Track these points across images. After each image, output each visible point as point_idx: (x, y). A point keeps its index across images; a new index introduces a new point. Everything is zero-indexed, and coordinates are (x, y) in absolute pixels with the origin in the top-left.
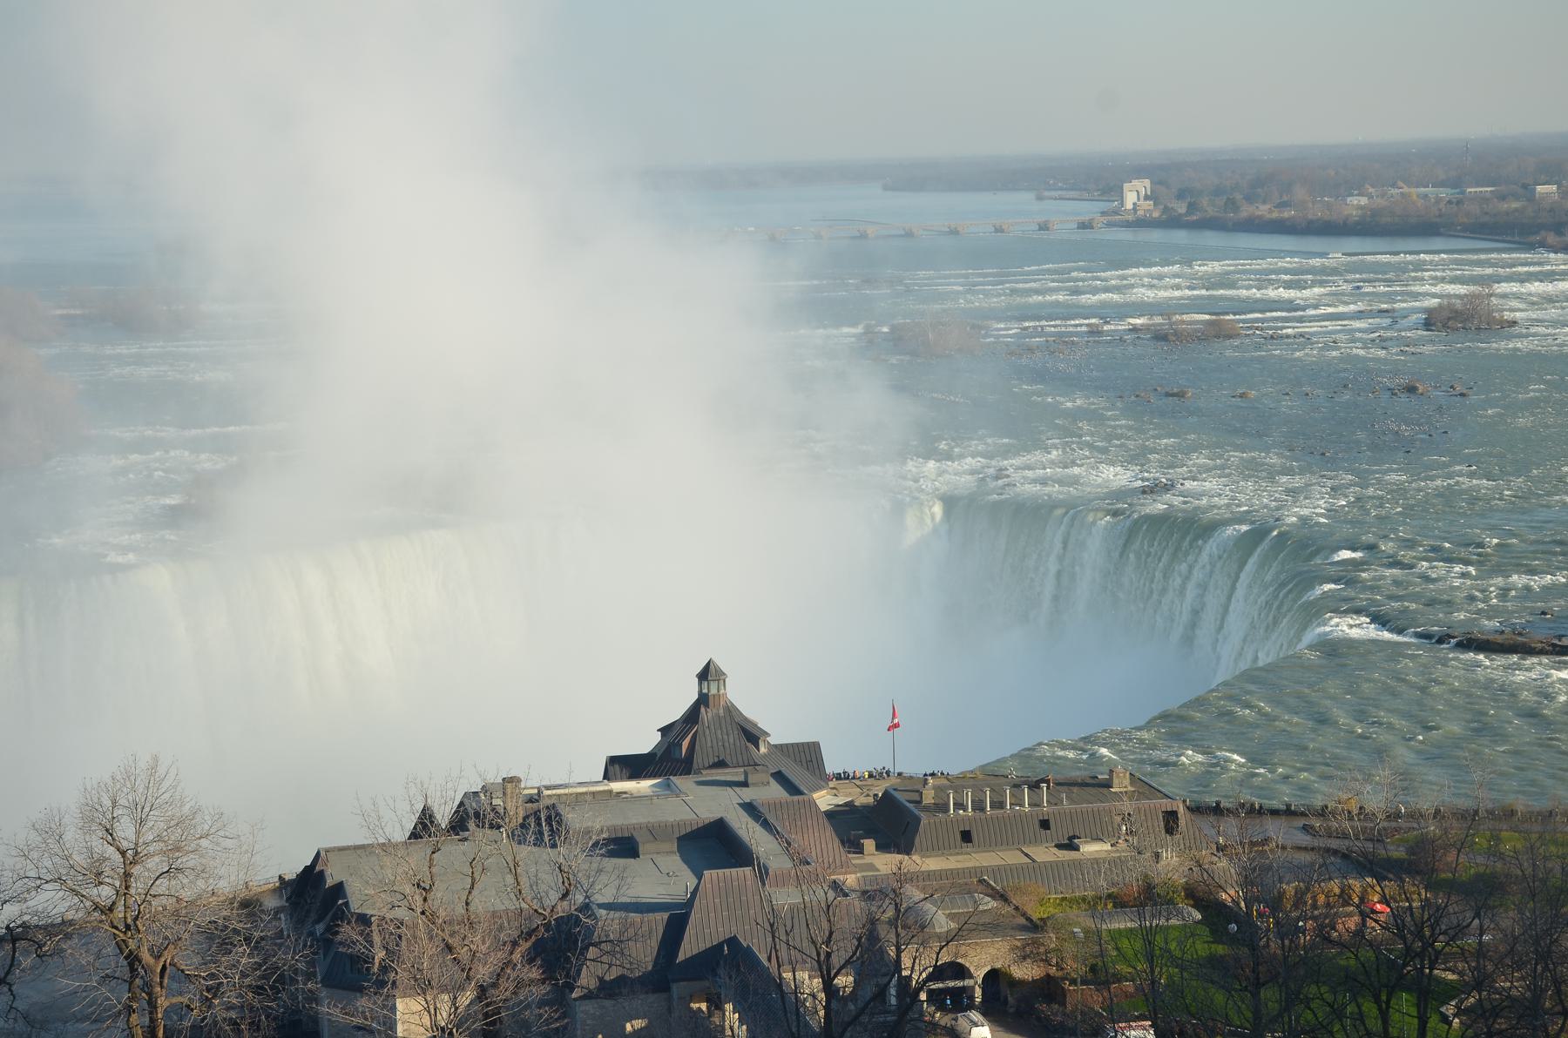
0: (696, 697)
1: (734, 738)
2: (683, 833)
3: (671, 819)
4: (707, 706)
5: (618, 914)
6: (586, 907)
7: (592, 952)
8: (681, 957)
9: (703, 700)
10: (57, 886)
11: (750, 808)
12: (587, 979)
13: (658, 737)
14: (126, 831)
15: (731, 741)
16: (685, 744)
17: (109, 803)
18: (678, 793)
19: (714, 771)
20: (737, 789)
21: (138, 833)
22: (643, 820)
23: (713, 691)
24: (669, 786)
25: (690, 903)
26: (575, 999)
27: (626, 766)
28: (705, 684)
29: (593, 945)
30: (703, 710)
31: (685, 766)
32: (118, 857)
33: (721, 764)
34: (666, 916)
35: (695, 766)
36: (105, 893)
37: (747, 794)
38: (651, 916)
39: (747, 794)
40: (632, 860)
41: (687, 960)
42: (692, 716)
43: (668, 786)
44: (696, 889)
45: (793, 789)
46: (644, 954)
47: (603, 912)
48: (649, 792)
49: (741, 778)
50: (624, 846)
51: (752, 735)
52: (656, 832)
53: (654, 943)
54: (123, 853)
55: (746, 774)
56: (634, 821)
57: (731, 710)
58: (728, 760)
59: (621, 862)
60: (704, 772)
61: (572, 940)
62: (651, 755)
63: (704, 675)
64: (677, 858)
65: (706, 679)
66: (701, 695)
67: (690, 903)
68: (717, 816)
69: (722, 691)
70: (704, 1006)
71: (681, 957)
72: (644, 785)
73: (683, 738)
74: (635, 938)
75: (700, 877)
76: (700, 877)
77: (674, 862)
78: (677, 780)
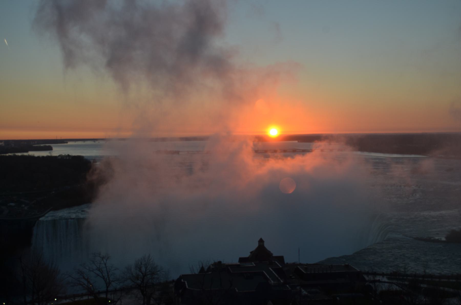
14: (143, 269)
17: (140, 263)
21: (146, 270)
32: (142, 275)
36: (139, 282)
54: (143, 274)
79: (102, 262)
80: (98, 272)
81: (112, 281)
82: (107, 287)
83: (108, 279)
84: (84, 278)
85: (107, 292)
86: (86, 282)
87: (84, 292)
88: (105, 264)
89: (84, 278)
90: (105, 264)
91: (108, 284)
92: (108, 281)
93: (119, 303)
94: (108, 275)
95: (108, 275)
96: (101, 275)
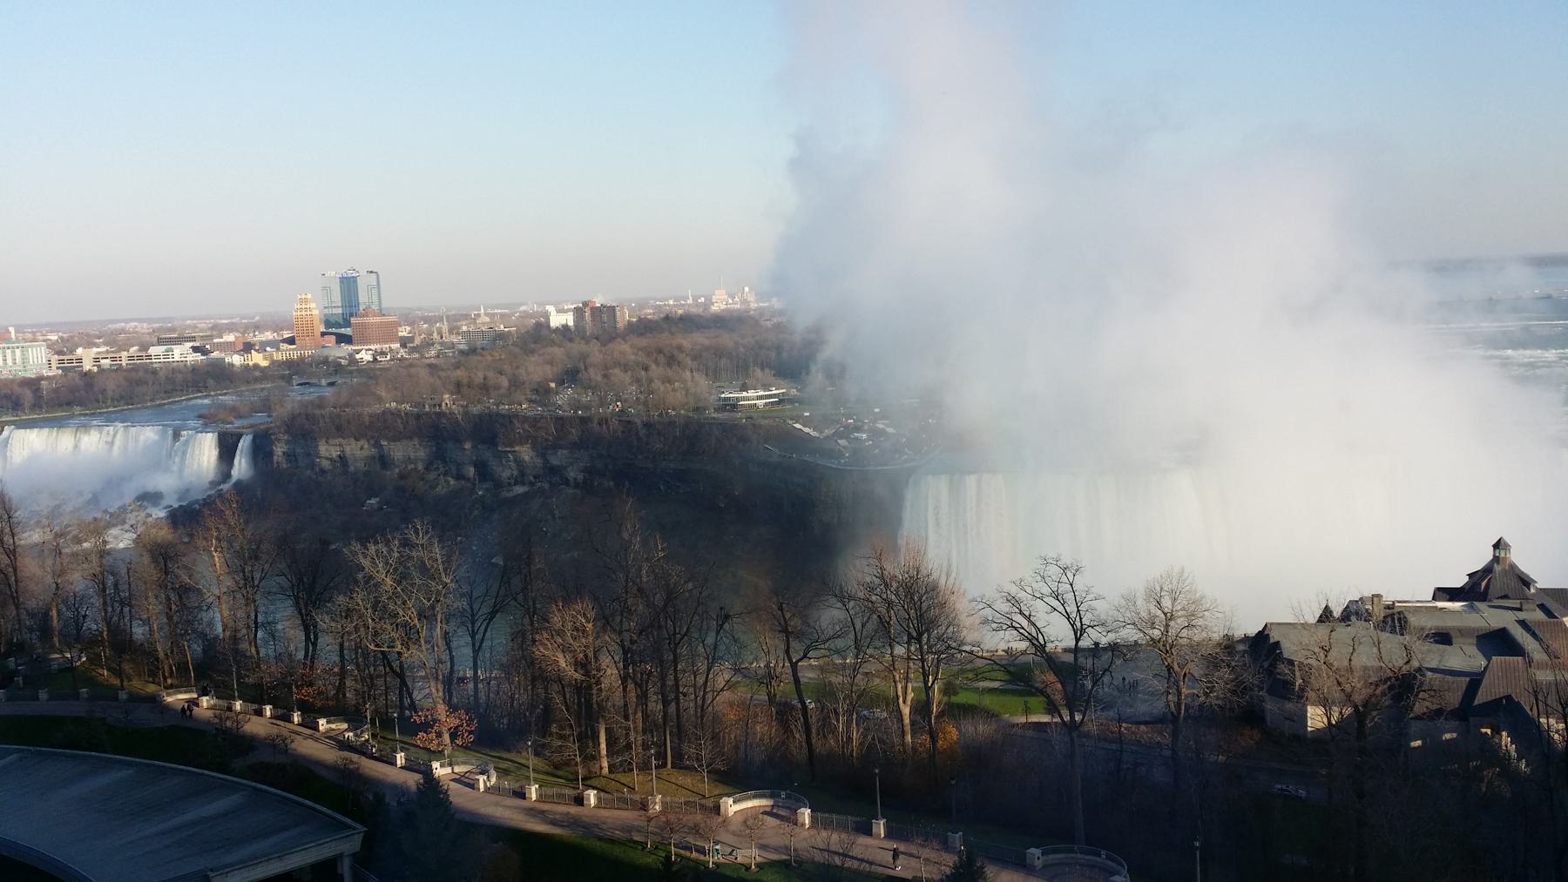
0: (1492, 557)
1: (1514, 583)
2: (1480, 633)
3: (1473, 626)
4: (1498, 563)
5: (1439, 675)
6: (1419, 670)
7: (1421, 695)
8: (1476, 703)
9: (1496, 559)
10: (1133, 626)
11: (1523, 624)
12: (1419, 708)
13: (1467, 579)
15: (1513, 584)
16: (1484, 584)
18: (1477, 611)
19: (1500, 601)
20: (1515, 612)
22: (1454, 624)
23: (1502, 555)
24: (1472, 606)
25: (1483, 673)
26: (1411, 718)
27: (1444, 593)
28: (1497, 551)
29: (1424, 691)
30: (1495, 565)
31: (1483, 597)
33: (1505, 597)
34: (1468, 679)
35: (1489, 597)
36: (1156, 633)
37: (1522, 615)
38: (1459, 679)
39: (1522, 615)
40: (1448, 646)
41: (1479, 705)
42: (1487, 570)
43: (1471, 607)
44: (1487, 666)
45: (1549, 614)
46: (1454, 699)
47: (1429, 674)
48: (1460, 609)
49: (1519, 606)
50: (1443, 638)
51: (1525, 582)
52: (1464, 632)
53: (1460, 694)
54: (1165, 614)
55: (1521, 603)
56: (1450, 625)
57: (1513, 567)
58: (1510, 595)
59: (1441, 646)
60: (1495, 601)
61: (1410, 688)
62: (1462, 588)
63: (1497, 546)
64: (1475, 648)
65: (1498, 548)
66: (1494, 556)
67: (1483, 673)
68: (1503, 626)
69: (1508, 556)
70: (1489, 731)
71: (1476, 703)
72: (1457, 605)
73: (1483, 580)
74: (1449, 690)
75: (1489, 660)
76: (1489, 660)
77: (1472, 650)
78: (1477, 604)
79: (1064, 579)
80: (1055, 603)
81: (1089, 626)
82: (1077, 640)
83: (1078, 618)
84: (1021, 613)
85: (1076, 650)
86: (1025, 623)
87: (1023, 645)
88: (1071, 585)
89: (1021, 613)
90: (1071, 585)
91: (1079, 633)
92: (1078, 624)
93: (1106, 679)
94: (1078, 611)
95: (1078, 611)
96: (1061, 609)
